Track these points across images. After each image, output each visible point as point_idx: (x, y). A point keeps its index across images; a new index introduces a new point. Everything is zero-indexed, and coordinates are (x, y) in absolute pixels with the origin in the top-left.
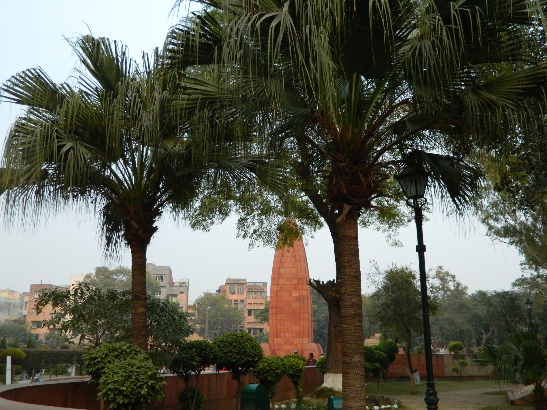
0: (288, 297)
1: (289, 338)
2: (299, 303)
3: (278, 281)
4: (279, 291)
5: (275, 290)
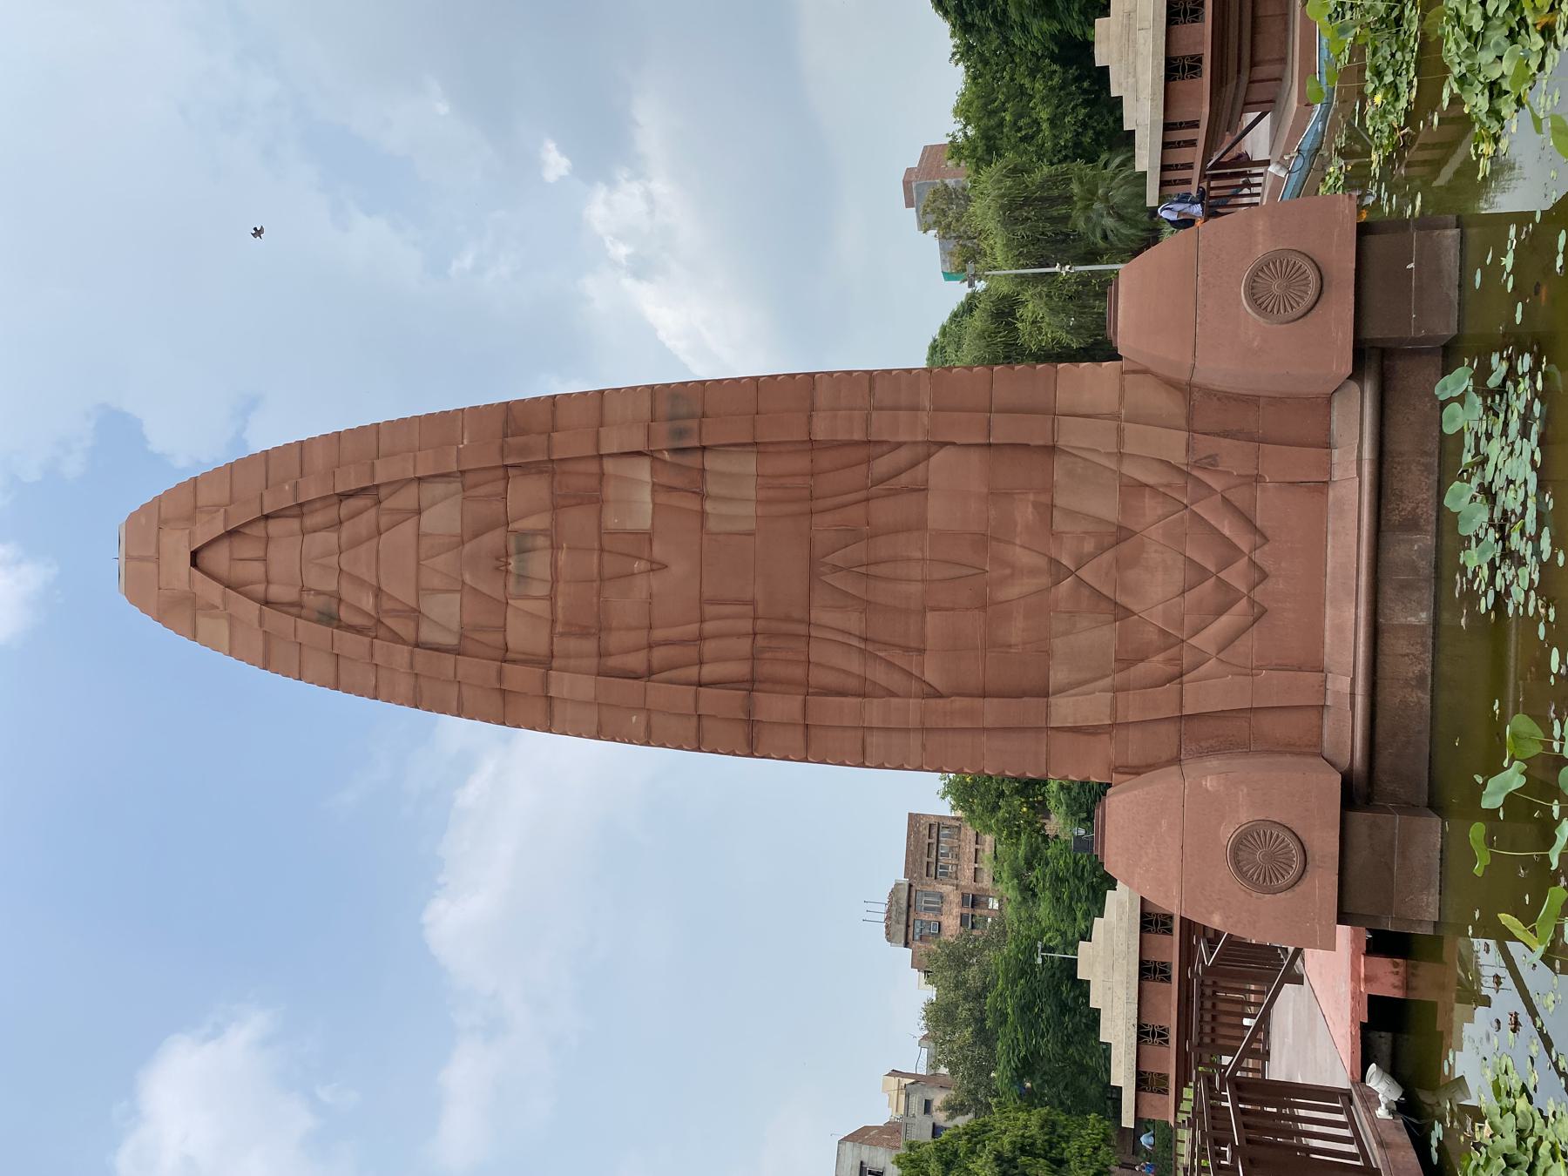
0: (657, 567)
2: (713, 462)
3: (528, 661)
4: (602, 654)
5: (585, 686)
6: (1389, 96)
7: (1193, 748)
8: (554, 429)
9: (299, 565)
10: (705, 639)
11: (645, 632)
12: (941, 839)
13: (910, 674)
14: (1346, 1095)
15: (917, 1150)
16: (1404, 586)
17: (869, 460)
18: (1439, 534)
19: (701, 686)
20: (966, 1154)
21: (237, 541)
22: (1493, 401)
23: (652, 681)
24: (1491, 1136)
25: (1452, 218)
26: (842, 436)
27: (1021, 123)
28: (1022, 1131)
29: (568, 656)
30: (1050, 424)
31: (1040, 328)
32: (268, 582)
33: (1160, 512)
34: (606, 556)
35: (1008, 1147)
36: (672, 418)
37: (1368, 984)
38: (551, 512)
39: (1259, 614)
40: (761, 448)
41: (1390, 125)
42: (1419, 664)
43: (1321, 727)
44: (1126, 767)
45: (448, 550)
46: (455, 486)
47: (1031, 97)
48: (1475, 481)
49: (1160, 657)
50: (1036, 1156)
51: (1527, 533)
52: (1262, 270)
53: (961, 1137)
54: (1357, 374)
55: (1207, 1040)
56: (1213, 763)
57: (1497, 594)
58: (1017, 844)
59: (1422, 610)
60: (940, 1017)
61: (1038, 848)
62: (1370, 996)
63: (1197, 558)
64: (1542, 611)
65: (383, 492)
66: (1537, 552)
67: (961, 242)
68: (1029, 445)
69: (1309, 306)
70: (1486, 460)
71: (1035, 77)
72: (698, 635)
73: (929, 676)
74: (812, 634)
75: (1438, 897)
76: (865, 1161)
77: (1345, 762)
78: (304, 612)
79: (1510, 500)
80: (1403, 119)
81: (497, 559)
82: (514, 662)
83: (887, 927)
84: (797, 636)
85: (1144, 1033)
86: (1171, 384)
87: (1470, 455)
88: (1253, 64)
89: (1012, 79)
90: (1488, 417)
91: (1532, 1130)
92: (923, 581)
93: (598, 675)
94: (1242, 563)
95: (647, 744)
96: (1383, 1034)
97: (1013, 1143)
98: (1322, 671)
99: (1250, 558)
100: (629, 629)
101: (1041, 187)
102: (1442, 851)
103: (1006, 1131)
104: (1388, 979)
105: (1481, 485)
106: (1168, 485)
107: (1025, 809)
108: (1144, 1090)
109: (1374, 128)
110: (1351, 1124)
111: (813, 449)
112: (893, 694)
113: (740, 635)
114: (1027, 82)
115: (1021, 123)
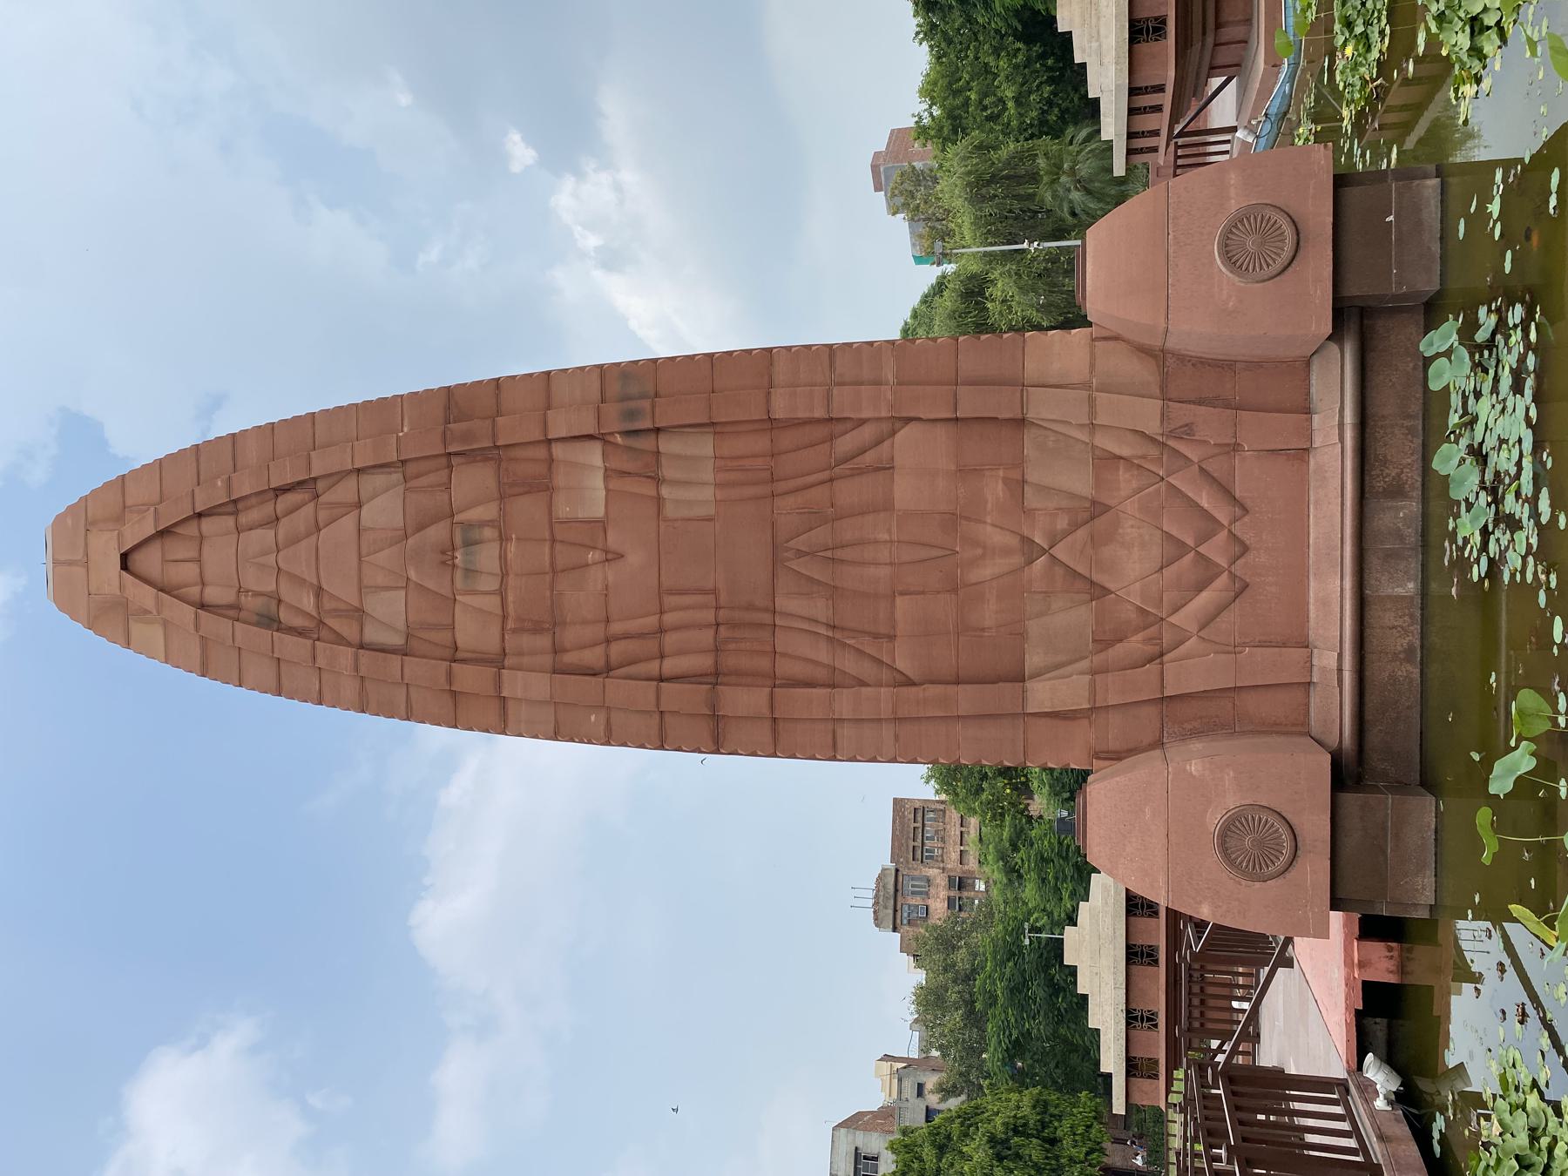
1: (1027, 541)
2: (668, 445)
3: (480, 660)
4: (557, 650)
6: (1360, 47)
7: (1176, 730)
8: (499, 413)
9: (235, 566)
10: (666, 631)
11: (602, 625)
12: (926, 822)
13: (880, 662)
14: (1342, 1085)
15: (912, 1135)
16: (1390, 555)
17: (832, 438)
18: (1425, 500)
19: (662, 680)
20: (959, 1137)
21: (169, 542)
22: (1481, 355)
23: (612, 677)
24: (1501, 1135)
25: (1431, 168)
26: (802, 414)
27: (986, 102)
28: (1014, 1112)
29: (520, 654)
30: (1018, 395)
31: (1010, 307)
32: (203, 584)
33: (1135, 484)
34: (558, 547)
35: (1000, 1128)
36: (626, 398)
37: (1363, 970)
38: (499, 502)
39: (1241, 589)
40: (718, 429)
41: (1362, 78)
42: (1408, 636)
43: (1307, 705)
44: (1107, 752)
45: (391, 546)
46: (397, 477)
47: (996, 75)
48: (1464, 442)
49: (1140, 636)
50: (1028, 1136)
51: (1523, 495)
52: (1236, 226)
53: (953, 1120)
54: (1336, 336)
55: (1196, 1024)
56: (1196, 746)
57: (1491, 561)
58: (1001, 826)
59: (1409, 580)
60: (930, 1001)
61: (1022, 830)
62: (1364, 982)
63: (1174, 533)
64: (1543, 577)
65: (321, 485)
66: (1535, 514)
67: (929, 224)
68: (997, 418)
69: (1286, 264)
70: (1475, 419)
71: (999, 55)
72: (658, 626)
73: (901, 664)
74: (777, 623)
75: (1433, 879)
76: (860, 1145)
77: (1333, 741)
78: (243, 615)
79: (1503, 461)
80: (1375, 69)
81: (443, 553)
82: (463, 661)
83: (875, 912)
84: (761, 625)
85: (1134, 1018)
86: (1144, 351)
87: (1457, 416)
88: (1218, 26)
89: (977, 58)
90: (1475, 374)
91: (1545, 1129)
92: (891, 564)
93: (554, 673)
94: (1223, 534)
95: (608, 743)
96: (1378, 1020)
97: (1005, 1124)
98: (1307, 647)
99: (1230, 531)
100: (585, 622)
101: (1008, 163)
102: (1436, 832)
103: (998, 1112)
104: (1382, 964)
105: (1470, 447)
106: (1144, 457)
107: (1008, 791)
108: (1134, 1076)
109: (1345, 83)
110: (1349, 1116)
111: (772, 428)
112: (862, 683)
113: (701, 626)
114: (991, 60)
115: (986, 102)
